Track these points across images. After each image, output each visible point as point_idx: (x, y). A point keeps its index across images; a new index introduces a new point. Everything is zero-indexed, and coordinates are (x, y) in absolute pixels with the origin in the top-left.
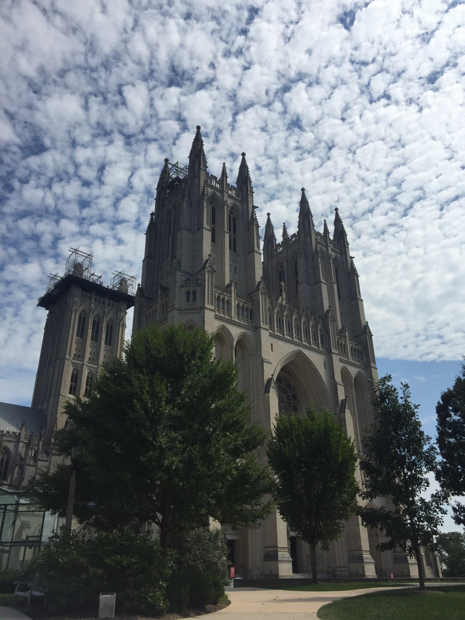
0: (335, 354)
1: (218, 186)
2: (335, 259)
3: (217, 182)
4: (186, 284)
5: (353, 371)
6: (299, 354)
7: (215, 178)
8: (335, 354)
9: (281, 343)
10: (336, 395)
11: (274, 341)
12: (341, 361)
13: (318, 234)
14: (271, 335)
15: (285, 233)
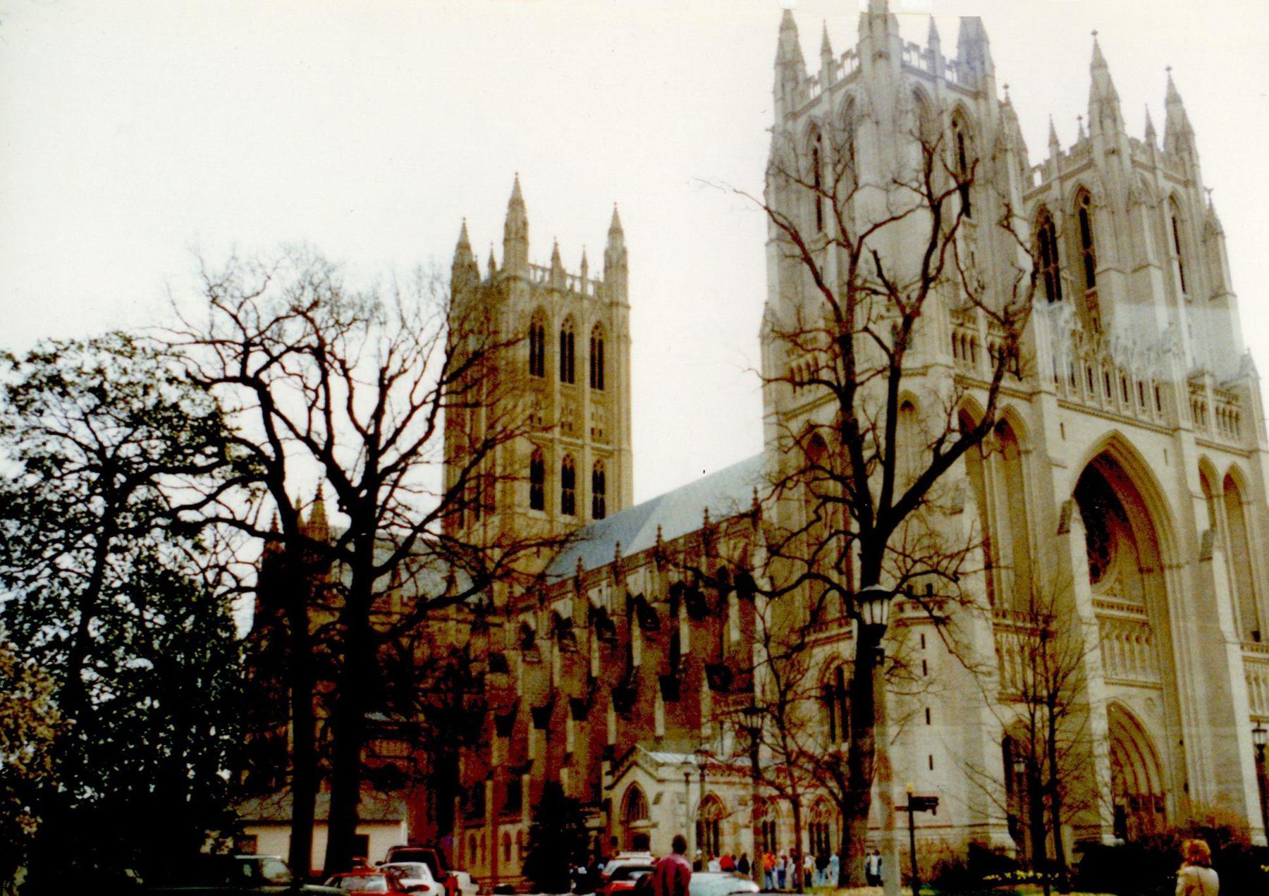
0: (1188, 430)
1: (923, 65)
2: (1172, 198)
3: (923, 57)
4: (888, 310)
5: (1221, 464)
6: (1115, 440)
7: (915, 47)
8: (1188, 430)
9: (1079, 418)
10: (1190, 520)
11: (1067, 414)
12: (1199, 443)
13: (1134, 143)
14: (1062, 404)
15: (1054, 142)
